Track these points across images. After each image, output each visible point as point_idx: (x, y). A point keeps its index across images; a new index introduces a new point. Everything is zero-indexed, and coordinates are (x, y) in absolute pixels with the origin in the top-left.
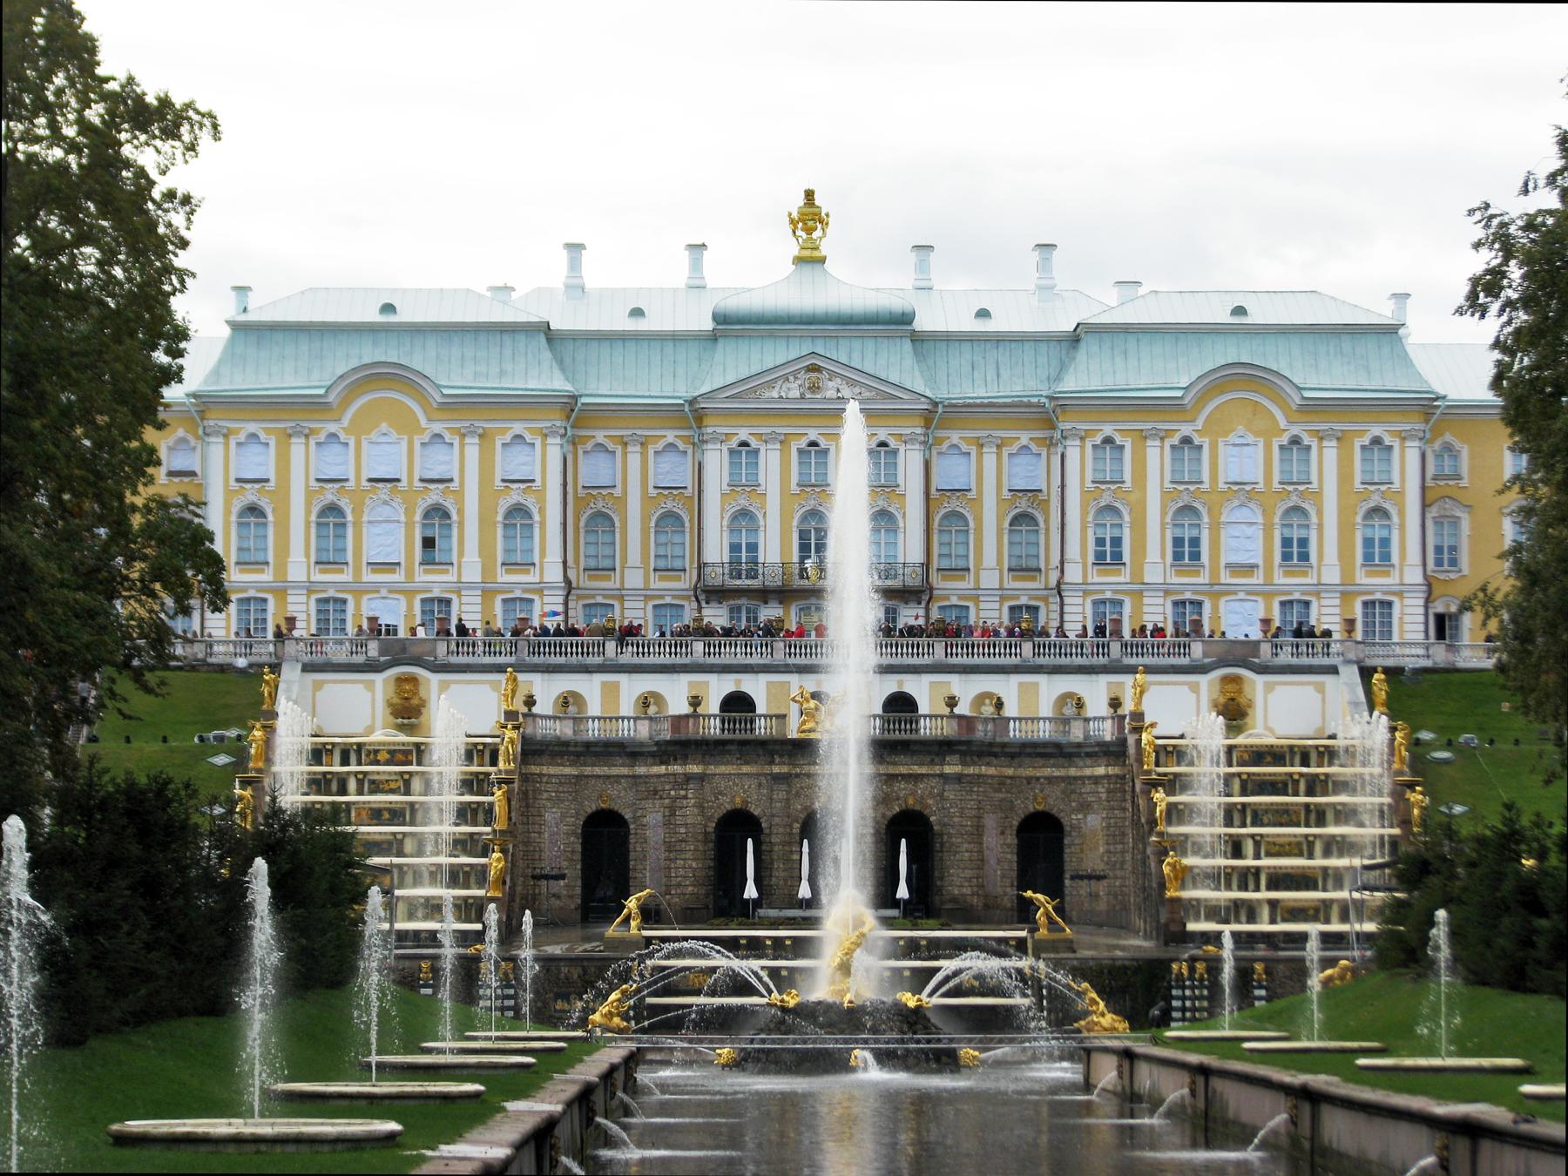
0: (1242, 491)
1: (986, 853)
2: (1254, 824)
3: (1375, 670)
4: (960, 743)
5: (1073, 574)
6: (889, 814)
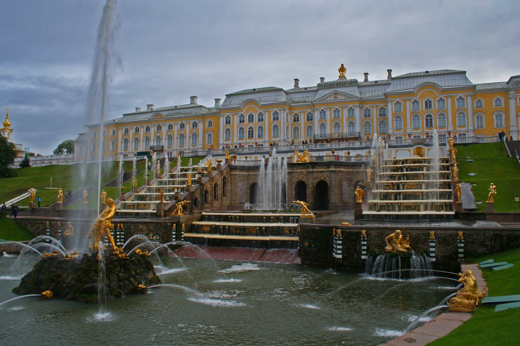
1: (343, 192)
2: (407, 179)
4: (333, 162)
6: (317, 182)
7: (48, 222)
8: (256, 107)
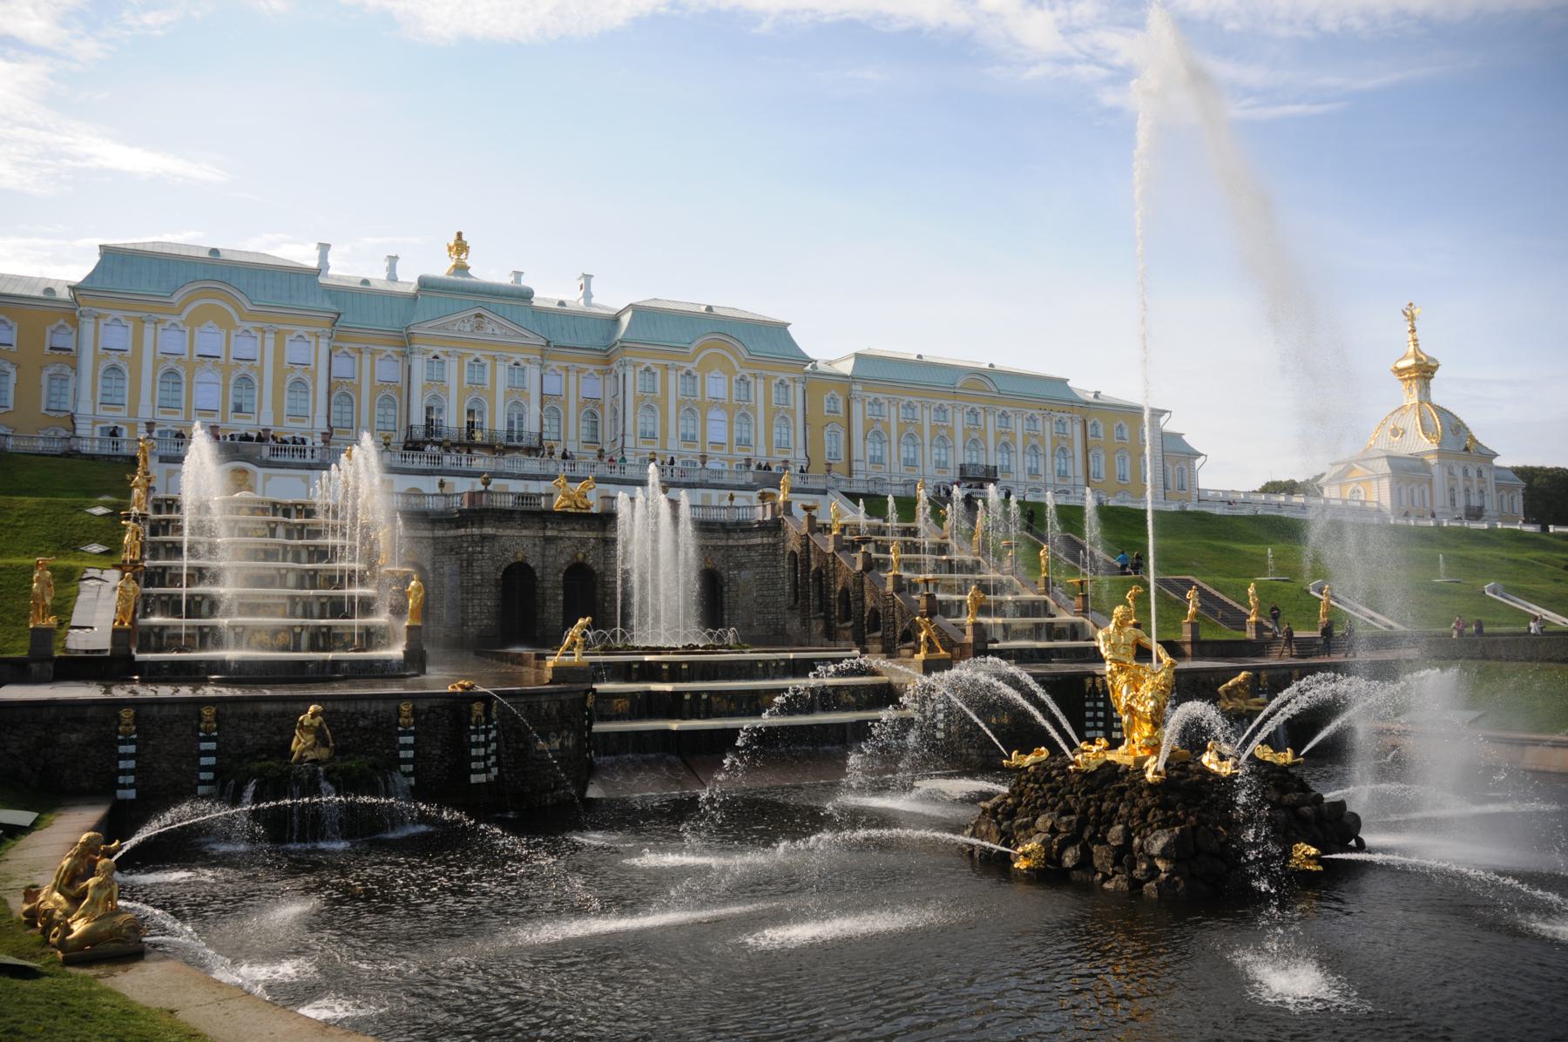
0: (716, 403)
5: (629, 442)
7: (126, 714)
8: (231, 310)
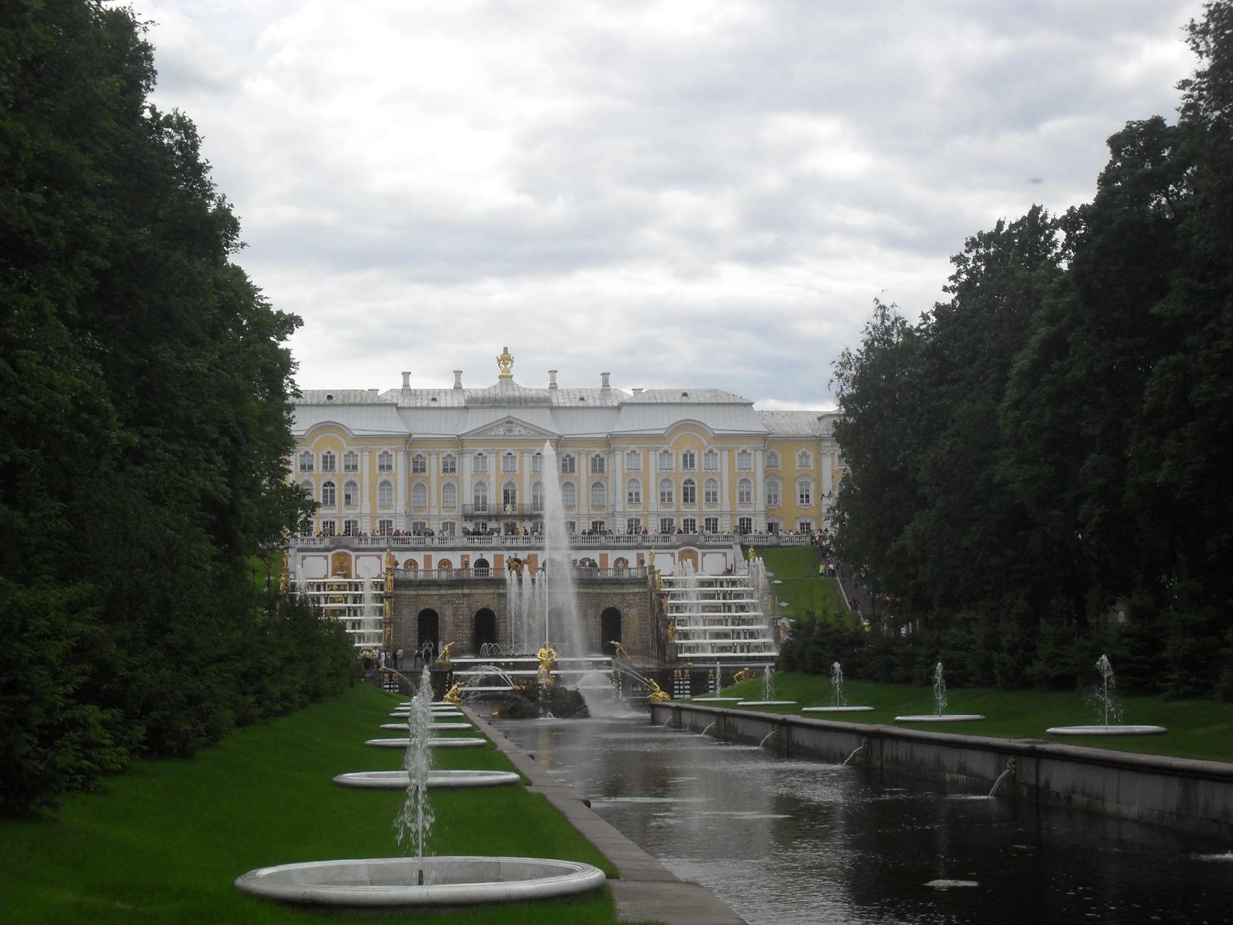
3: (749, 547)
5: (619, 508)
